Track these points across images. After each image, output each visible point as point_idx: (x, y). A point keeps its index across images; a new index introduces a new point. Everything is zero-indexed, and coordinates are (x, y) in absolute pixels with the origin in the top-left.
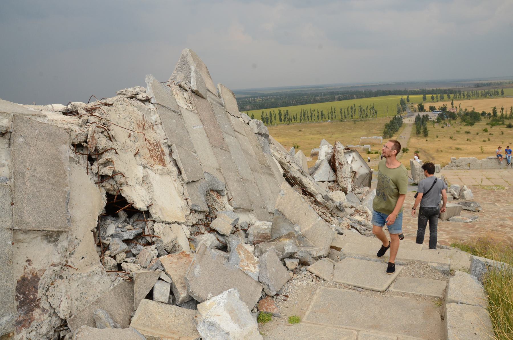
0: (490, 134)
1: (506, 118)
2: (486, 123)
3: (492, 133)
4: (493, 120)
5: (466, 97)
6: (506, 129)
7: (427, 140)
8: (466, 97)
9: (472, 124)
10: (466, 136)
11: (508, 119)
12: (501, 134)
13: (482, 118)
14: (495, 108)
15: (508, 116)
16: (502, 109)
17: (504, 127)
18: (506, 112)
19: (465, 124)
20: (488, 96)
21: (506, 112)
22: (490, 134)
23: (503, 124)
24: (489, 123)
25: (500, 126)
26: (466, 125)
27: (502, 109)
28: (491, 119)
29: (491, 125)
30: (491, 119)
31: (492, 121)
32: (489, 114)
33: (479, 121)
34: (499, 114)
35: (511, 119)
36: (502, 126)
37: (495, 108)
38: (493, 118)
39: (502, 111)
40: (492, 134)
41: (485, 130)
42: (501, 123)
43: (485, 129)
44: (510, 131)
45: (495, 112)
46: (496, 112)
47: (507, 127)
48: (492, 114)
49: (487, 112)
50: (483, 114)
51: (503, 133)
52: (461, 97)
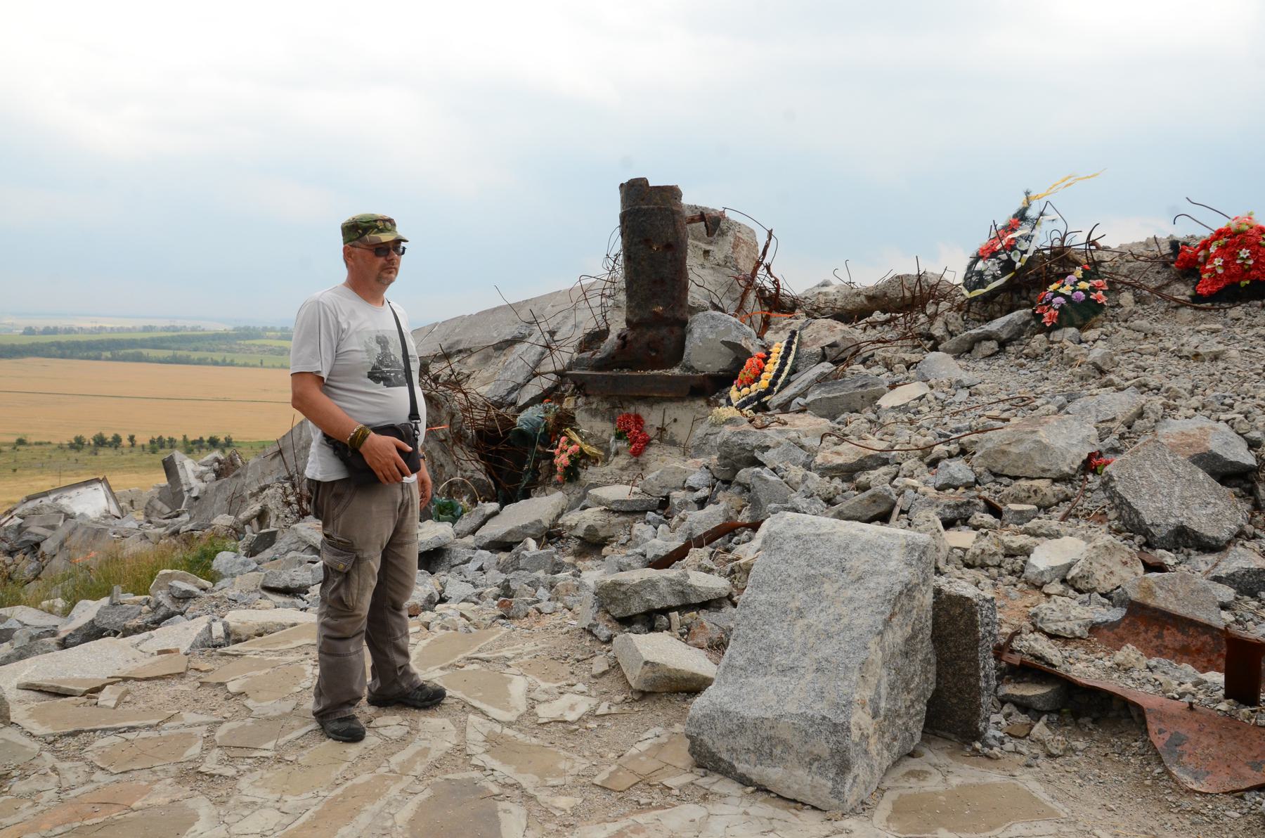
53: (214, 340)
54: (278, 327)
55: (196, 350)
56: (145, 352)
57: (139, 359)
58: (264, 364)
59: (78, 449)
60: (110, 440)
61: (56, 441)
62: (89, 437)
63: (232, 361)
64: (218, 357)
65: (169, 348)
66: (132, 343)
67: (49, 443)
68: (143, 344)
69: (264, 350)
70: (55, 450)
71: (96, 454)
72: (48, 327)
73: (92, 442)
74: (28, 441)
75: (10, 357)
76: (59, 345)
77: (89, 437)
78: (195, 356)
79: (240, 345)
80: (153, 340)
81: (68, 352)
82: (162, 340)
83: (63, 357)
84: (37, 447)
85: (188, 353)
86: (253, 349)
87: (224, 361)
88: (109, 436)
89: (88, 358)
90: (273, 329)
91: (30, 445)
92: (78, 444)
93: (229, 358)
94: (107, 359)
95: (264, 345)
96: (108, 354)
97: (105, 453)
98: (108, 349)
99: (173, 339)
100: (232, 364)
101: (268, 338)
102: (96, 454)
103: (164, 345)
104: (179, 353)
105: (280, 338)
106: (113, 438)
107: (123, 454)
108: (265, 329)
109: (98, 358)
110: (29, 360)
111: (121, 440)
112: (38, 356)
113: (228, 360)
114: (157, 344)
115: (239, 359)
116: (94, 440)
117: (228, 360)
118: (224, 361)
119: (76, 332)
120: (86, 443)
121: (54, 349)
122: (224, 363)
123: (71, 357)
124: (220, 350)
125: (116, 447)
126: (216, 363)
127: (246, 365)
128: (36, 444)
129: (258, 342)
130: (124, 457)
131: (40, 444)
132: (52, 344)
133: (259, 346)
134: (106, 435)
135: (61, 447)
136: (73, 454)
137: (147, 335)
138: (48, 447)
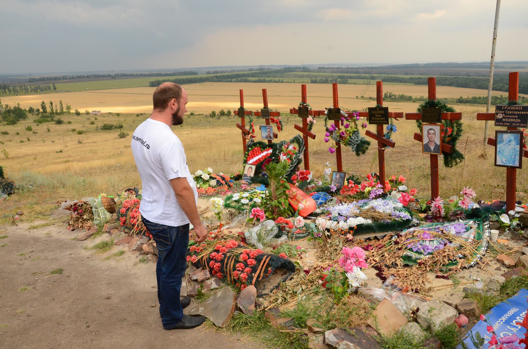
0: (34, 133)
1: (57, 113)
2: (32, 121)
3: (36, 131)
4: (42, 117)
5: (12, 93)
6: (55, 125)
7: (80, 143)
8: (12, 93)
9: (13, 123)
10: (17, 138)
11: (59, 115)
12: (48, 131)
13: (29, 115)
14: (43, 103)
15: (59, 111)
16: (51, 103)
17: (52, 124)
18: (56, 107)
19: (5, 123)
20: (39, 91)
21: (56, 107)
22: (34, 133)
23: (52, 120)
24: (36, 120)
25: (49, 123)
26: (8, 124)
27: (51, 103)
28: (40, 115)
29: (38, 122)
30: (40, 115)
31: (41, 118)
32: (38, 110)
33: (25, 118)
34: (49, 110)
35: (62, 114)
36: (51, 123)
37: (43, 103)
38: (42, 114)
39: (52, 106)
40: (37, 133)
41: (29, 129)
42: (50, 119)
43: (28, 128)
44: (59, 128)
45: (44, 108)
46: (46, 108)
47: (56, 124)
48: (41, 110)
49: (35, 108)
50: (31, 110)
51: (49, 131)
52: (6, 93)
53: (276, 73)
54: (301, 67)
55: (268, 77)
56: (248, 78)
57: (246, 81)
58: (295, 81)
59: (213, 117)
60: (226, 113)
61: (205, 114)
62: (217, 112)
63: (282, 80)
64: (277, 79)
65: (258, 77)
66: (244, 75)
67: (203, 114)
68: (248, 75)
69: (295, 76)
70: (203, 117)
71: (219, 119)
72: (215, 71)
73: (219, 114)
74: (195, 113)
75: (200, 82)
76: (217, 77)
77: (217, 112)
78: (267, 79)
79: (286, 74)
80: (252, 73)
81: (220, 79)
82: (255, 73)
83: (218, 81)
84: (197, 116)
85: (264, 78)
86: (291, 76)
87: (279, 81)
88: (226, 111)
89: (228, 82)
90: (299, 68)
91: (195, 115)
92: (213, 115)
93: (281, 79)
94: (234, 82)
95: (295, 74)
96: (235, 80)
97: (225, 118)
98: (235, 78)
99: (260, 73)
100: (282, 82)
101: (297, 71)
102: (219, 119)
103: (256, 75)
104: (261, 78)
105: (302, 71)
106: (228, 112)
107: (230, 118)
108: (296, 68)
109: (231, 81)
110: (198, 84)
111: (231, 113)
112: (210, 81)
113: (281, 81)
114: (253, 75)
115: (285, 80)
116: (220, 113)
117: (281, 81)
118: (279, 81)
119: (225, 73)
120: (217, 114)
121: (215, 78)
122: (279, 82)
123: (221, 81)
124: (278, 77)
125: (228, 116)
126: (276, 82)
127: (288, 82)
128: (198, 115)
129: (293, 73)
130: (230, 120)
131: (200, 115)
132: (215, 77)
133: (294, 75)
134: (225, 111)
135: (206, 116)
136: (211, 119)
137: (250, 72)
138: (203, 116)
